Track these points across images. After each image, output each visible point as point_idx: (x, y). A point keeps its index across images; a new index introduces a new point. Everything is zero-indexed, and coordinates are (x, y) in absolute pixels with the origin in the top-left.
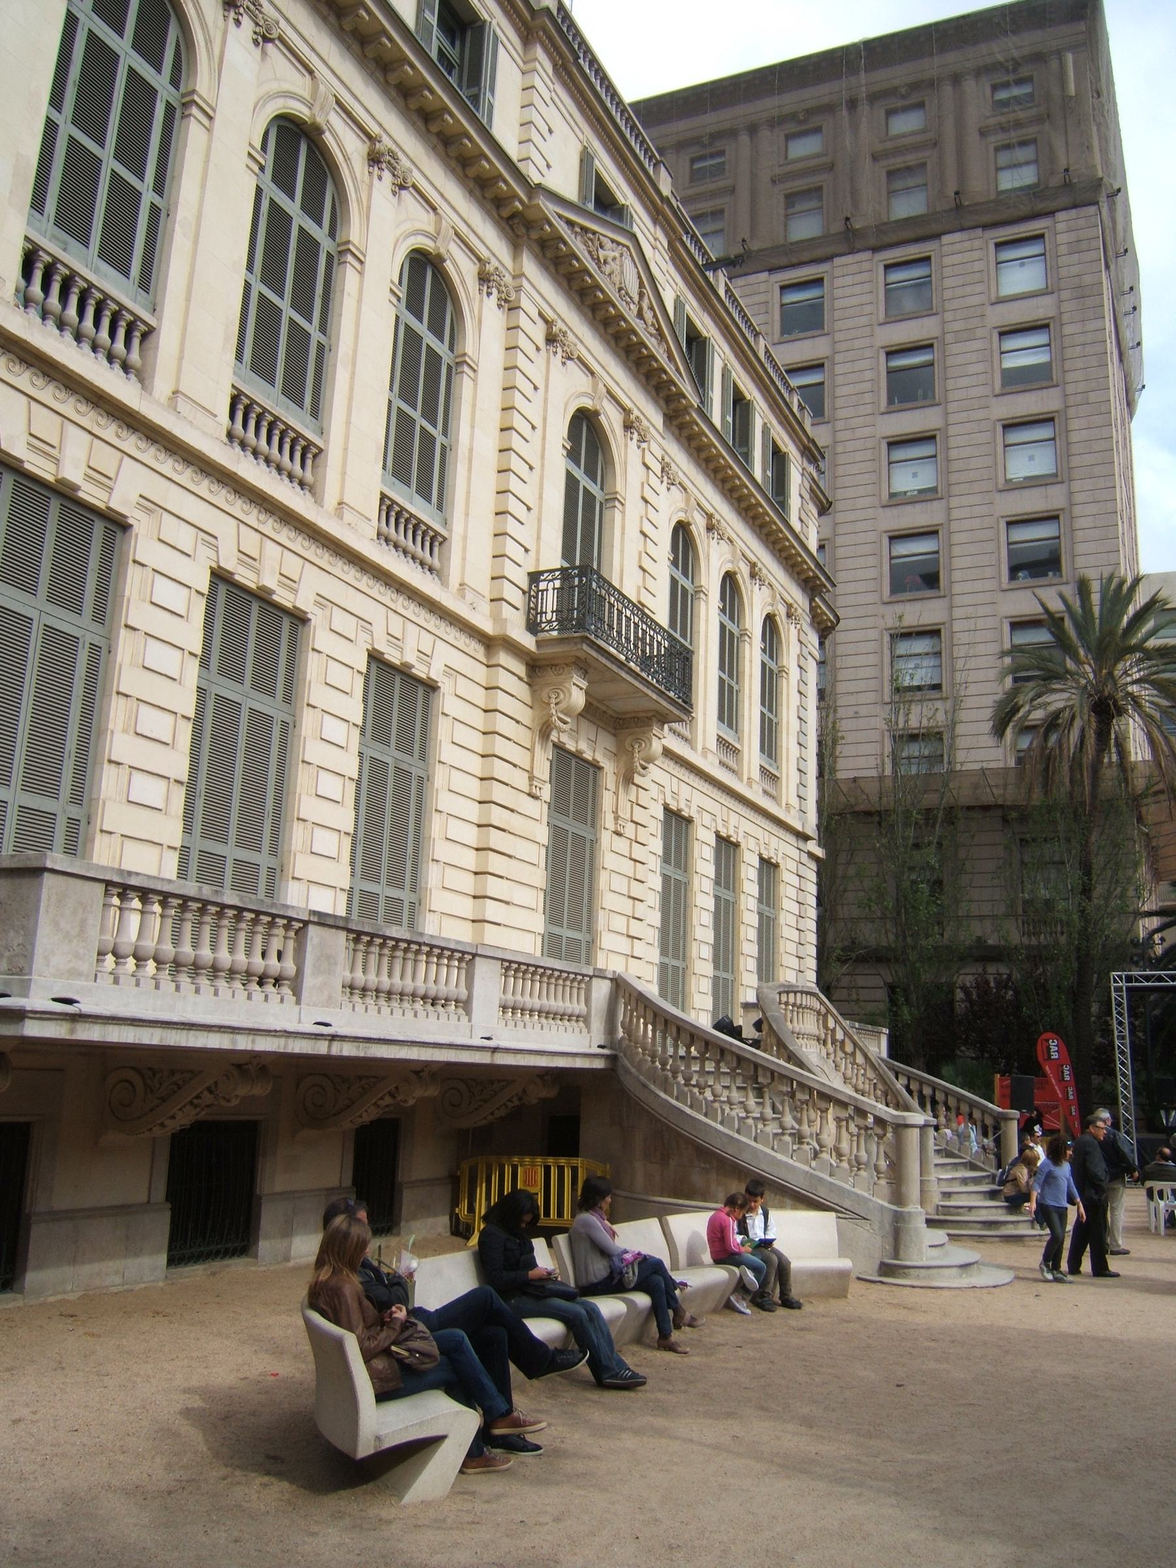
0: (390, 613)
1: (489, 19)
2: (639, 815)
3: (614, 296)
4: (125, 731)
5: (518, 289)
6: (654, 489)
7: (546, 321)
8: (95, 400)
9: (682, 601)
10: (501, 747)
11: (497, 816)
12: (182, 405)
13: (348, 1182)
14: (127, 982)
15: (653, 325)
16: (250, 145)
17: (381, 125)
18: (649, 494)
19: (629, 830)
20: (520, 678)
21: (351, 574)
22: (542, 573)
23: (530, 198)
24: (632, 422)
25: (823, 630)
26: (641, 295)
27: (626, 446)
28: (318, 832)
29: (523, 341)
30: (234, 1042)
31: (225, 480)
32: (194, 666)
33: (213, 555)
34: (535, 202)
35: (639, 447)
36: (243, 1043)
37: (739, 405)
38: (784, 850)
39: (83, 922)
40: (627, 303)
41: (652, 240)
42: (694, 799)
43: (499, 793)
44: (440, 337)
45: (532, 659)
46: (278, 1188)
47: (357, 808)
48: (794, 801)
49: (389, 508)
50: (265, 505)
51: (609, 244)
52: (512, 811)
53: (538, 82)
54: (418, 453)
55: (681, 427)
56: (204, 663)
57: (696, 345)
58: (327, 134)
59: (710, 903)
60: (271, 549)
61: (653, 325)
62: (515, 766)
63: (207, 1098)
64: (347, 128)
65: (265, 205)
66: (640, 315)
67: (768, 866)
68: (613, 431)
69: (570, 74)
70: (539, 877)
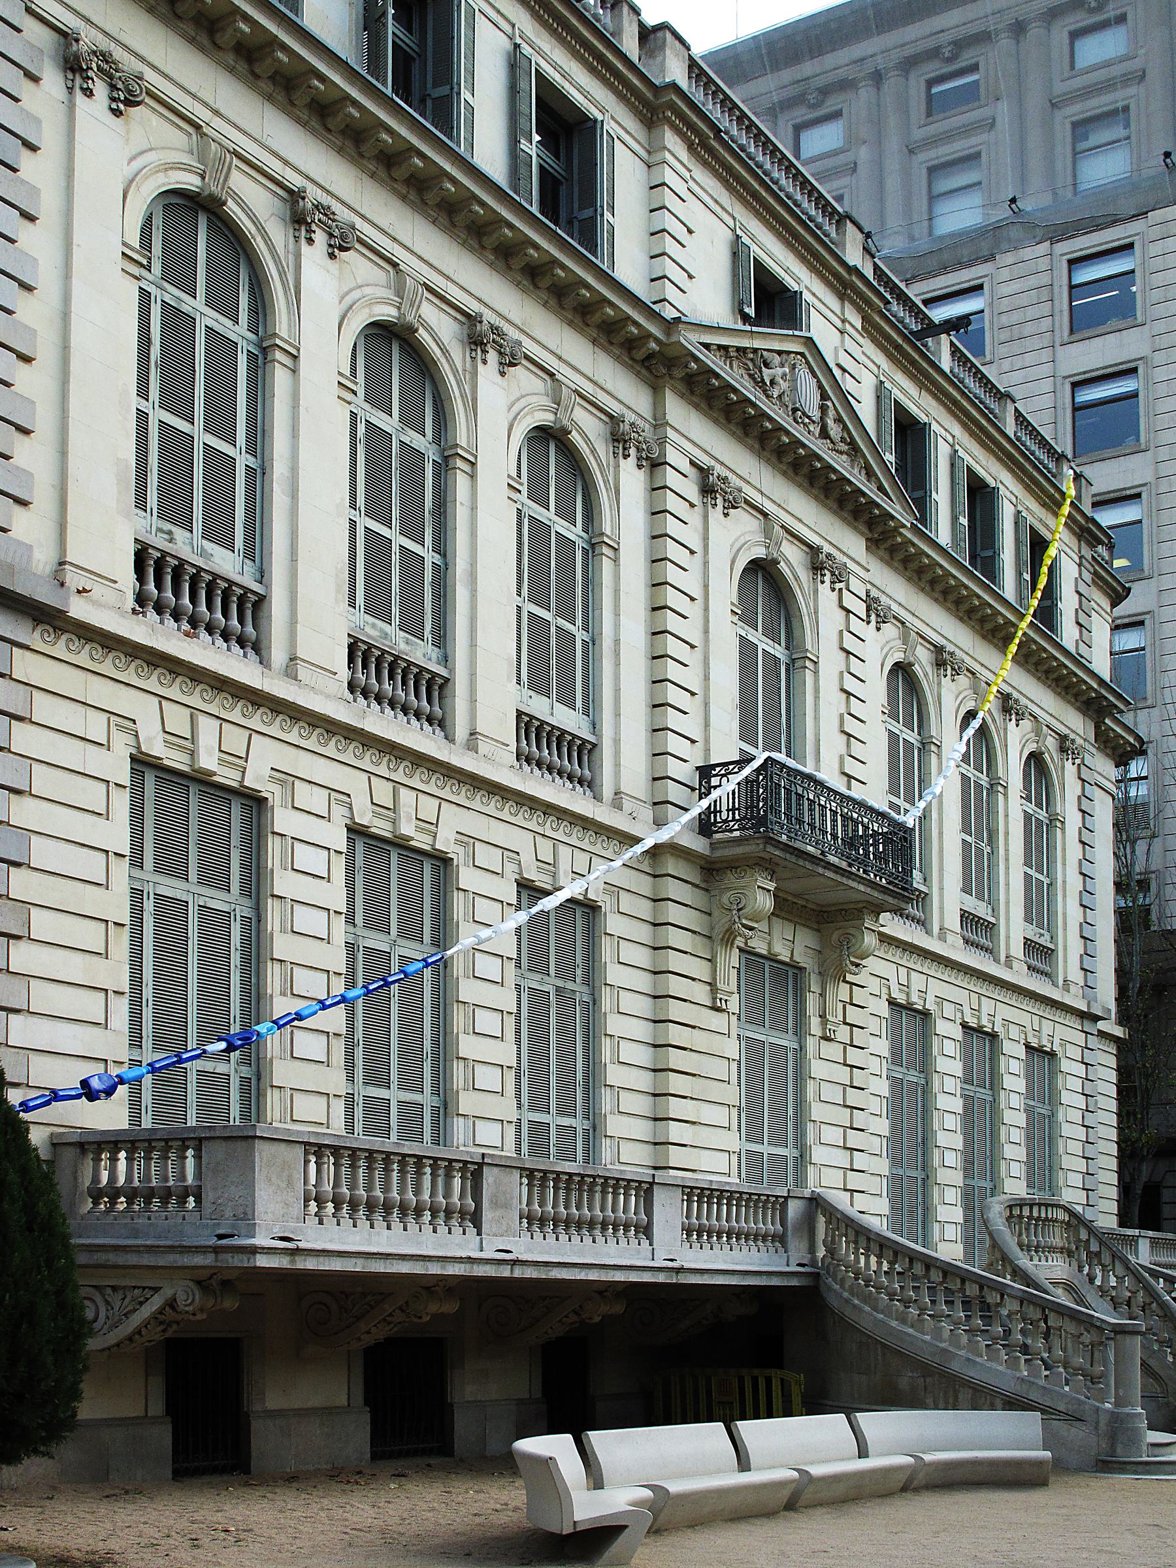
0: (538, 838)
1: (600, 117)
2: (853, 1015)
3: (786, 422)
4: (283, 994)
5: (662, 441)
6: (857, 633)
7: (700, 469)
8: (219, 685)
10: (675, 961)
12: (303, 672)
13: (538, 1394)
14: (330, 1222)
15: (843, 440)
16: (340, 373)
17: (480, 300)
18: (850, 643)
19: (843, 1033)
20: (697, 886)
23: (668, 333)
24: (822, 563)
25: (1121, 756)
26: (823, 409)
27: (816, 591)
28: (479, 1069)
29: (672, 503)
30: (427, 1269)
31: (352, 736)
32: (339, 924)
34: (674, 339)
35: (833, 590)
36: (434, 1269)
37: (979, 497)
38: (1064, 1035)
39: (290, 1176)
40: (805, 424)
41: (839, 324)
42: (930, 989)
43: (676, 1010)
45: (707, 862)
47: (518, 1042)
48: (1076, 976)
49: (528, 725)
51: (777, 359)
52: (694, 1027)
53: (670, 177)
55: (892, 551)
57: (910, 433)
58: (421, 331)
59: (957, 1105)
61: (843, 440)
62: (694, 979)
64: (442, 315)
65: (361, 429)
66: (824, 434)
67: (1041, 1056)
68: (797, 578)
69: (711, 151)
70: (732, 1094)
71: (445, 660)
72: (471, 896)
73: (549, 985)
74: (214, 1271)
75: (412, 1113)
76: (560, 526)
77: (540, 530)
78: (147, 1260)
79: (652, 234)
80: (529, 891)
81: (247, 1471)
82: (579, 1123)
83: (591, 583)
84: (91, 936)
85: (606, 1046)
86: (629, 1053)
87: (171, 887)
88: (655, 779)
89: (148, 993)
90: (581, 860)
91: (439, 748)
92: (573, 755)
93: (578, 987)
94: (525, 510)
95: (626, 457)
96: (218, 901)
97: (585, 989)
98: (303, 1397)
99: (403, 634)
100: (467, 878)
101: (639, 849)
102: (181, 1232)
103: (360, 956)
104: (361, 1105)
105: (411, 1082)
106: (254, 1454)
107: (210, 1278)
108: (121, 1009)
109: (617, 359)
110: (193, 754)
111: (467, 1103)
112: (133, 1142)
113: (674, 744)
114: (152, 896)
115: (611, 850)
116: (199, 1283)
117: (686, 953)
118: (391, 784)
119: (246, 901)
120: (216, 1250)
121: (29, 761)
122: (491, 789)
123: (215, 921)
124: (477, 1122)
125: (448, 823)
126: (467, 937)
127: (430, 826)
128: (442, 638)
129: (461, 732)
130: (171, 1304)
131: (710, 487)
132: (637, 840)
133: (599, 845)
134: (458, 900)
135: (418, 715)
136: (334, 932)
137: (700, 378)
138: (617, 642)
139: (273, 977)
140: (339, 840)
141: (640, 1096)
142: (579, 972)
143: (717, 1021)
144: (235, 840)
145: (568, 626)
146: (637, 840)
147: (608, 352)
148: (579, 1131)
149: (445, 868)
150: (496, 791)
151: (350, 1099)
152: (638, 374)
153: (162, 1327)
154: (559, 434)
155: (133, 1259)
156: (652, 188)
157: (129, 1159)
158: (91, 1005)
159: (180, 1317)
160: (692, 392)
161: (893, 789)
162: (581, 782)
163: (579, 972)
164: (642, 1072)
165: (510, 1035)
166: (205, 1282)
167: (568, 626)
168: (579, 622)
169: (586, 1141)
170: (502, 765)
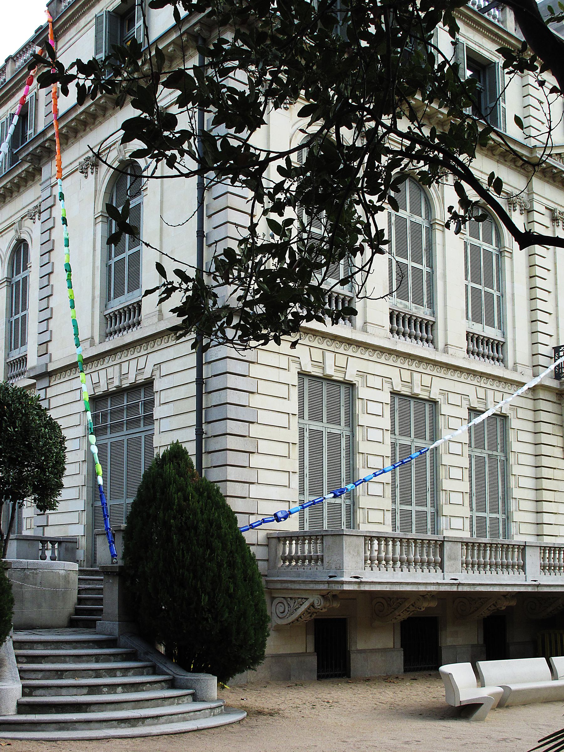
0: (478, 388)
4: (364, 467)
5: (531, 201)
10: (544, 439)
11: (545, 473)
13: (481, 642)
20: (555, 403)
21: (456, 376)
22: (560, 347)
32: (388, 435)
33: (390, 386)
43: (545, 461)
46: (449, 644)
50: (411, 358)
56: (393, 432)
60: (416, 376)
63: (412, 608)
71: (433, 314)
72: (447, 417)
73: (485, 453)
74: (329, 592)
75: (421, 515)
76: (485, 246)
77: (475, 249)
78: (303, 587)
79: (524, 107)
80: (474, 412)
81: (349, 677)
82: (500, 516)
83: (500, 269)
84: (282, 449)
85: (512, 480)
86: (523, 482)
87: (316, 426)
88: (533, 355)
89: (307, 471)
90: (498, 396)
91: (430, 354)
92: (495, 349)
93: (499, 454)
94: (468, 242)
95: (514, 210)
96: (335, 429)
97: (502, 454)
98: (374, 644)
99: (414, 305)
100: (445, 409)
101: (525, 388)
102: (316, 575)
103: (398, 448)
104: (399, 513)
105: (421, 502)
106: (352, 669)
107: (328, 594)
108: (295, 479)
109: (509, 167)
110: (323, 368)
111: (446, 510)
112: (298, 537)
113: (541, 338)
114: (308, 430)
115: (513, 390)
116: (323, 596)
117: (550, 434)
118: (410, 372)
119: (348, 429)
120: (329, 583)
121: (257, 380)
122: (455, 369)
123: (334, 438)
124: (452, 518)
125: (435, 385)
126: (446, 435)
127: (428, 388)
128: (431, 304)
129: (441, 345)
130: (312, 605)
132: (524, 384)
133: (507, 388)
134: (441, 420)
135: (421, 340)
136: (385, 438)
137: (548, 169)
138: (513, 295)
139: (359, 460)
140: (387, 398)
141: (530, 502)
142: (499, 447)
144: (342, 403)
145: (490, 290)
146: (524, 384)
147: (505, 165)
148: (501, 520)
149: (435, 405)
150: (457, 369)
151: (394, 511)
152: (519, 172)
153: (310, 615)
154: (483, 206)
155: (297, 586)
156: (523, 86)
157: (297, 544)
158: (283, 479)
159: (316, 611)
160: (545, 176)
162: (498, 360)
163: (499, 447)
164: (530, 491)
165: (466, 478)
166: (326, 596)
167: (490, 290)
168: (495, 288)
169: (504, 524)
170: (459, 358)
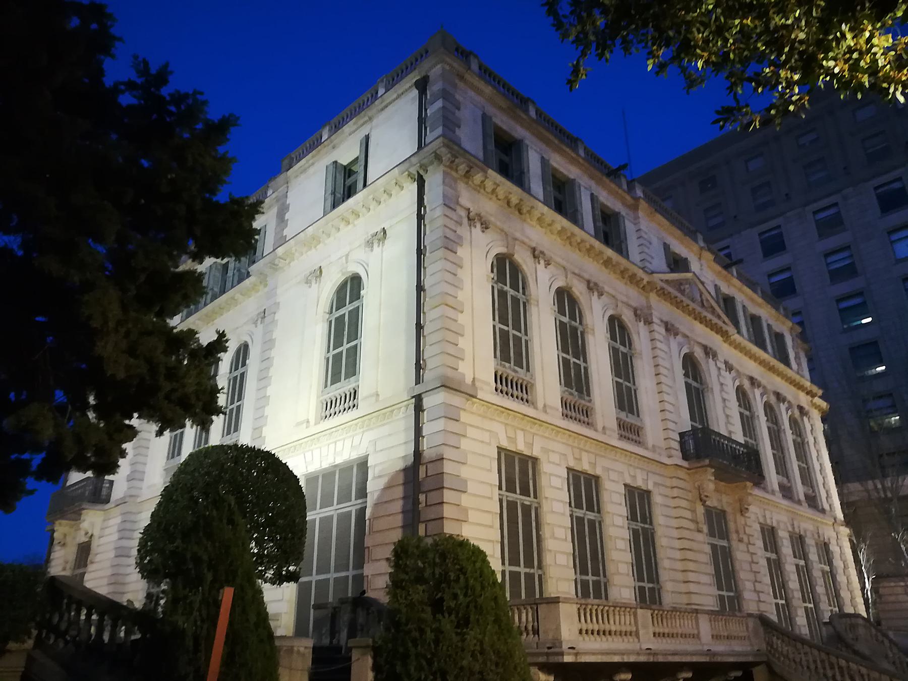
9: (748, 423)
44: (625, 346)
54: (626, 400)
131: (670, 329)
143: (700, 537)
161: (745, 435)
